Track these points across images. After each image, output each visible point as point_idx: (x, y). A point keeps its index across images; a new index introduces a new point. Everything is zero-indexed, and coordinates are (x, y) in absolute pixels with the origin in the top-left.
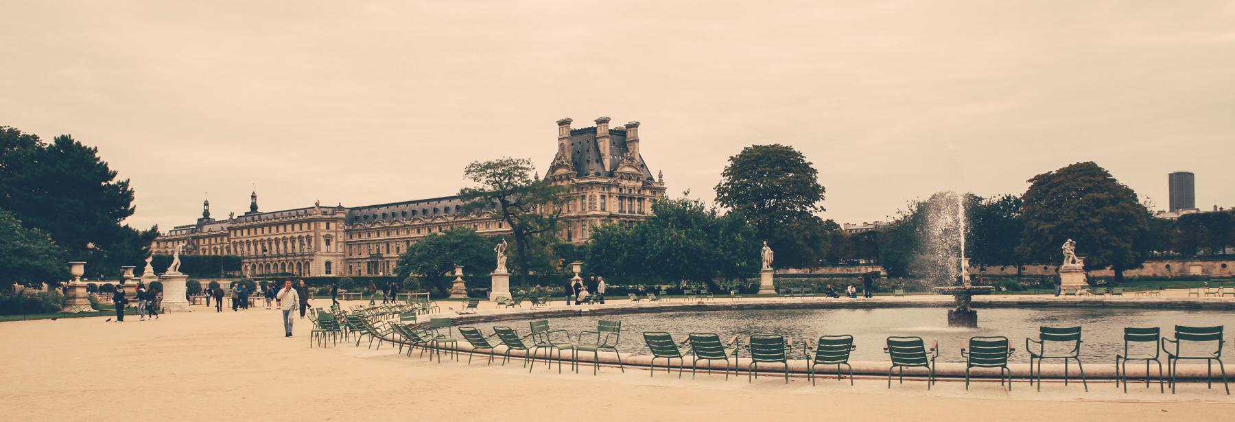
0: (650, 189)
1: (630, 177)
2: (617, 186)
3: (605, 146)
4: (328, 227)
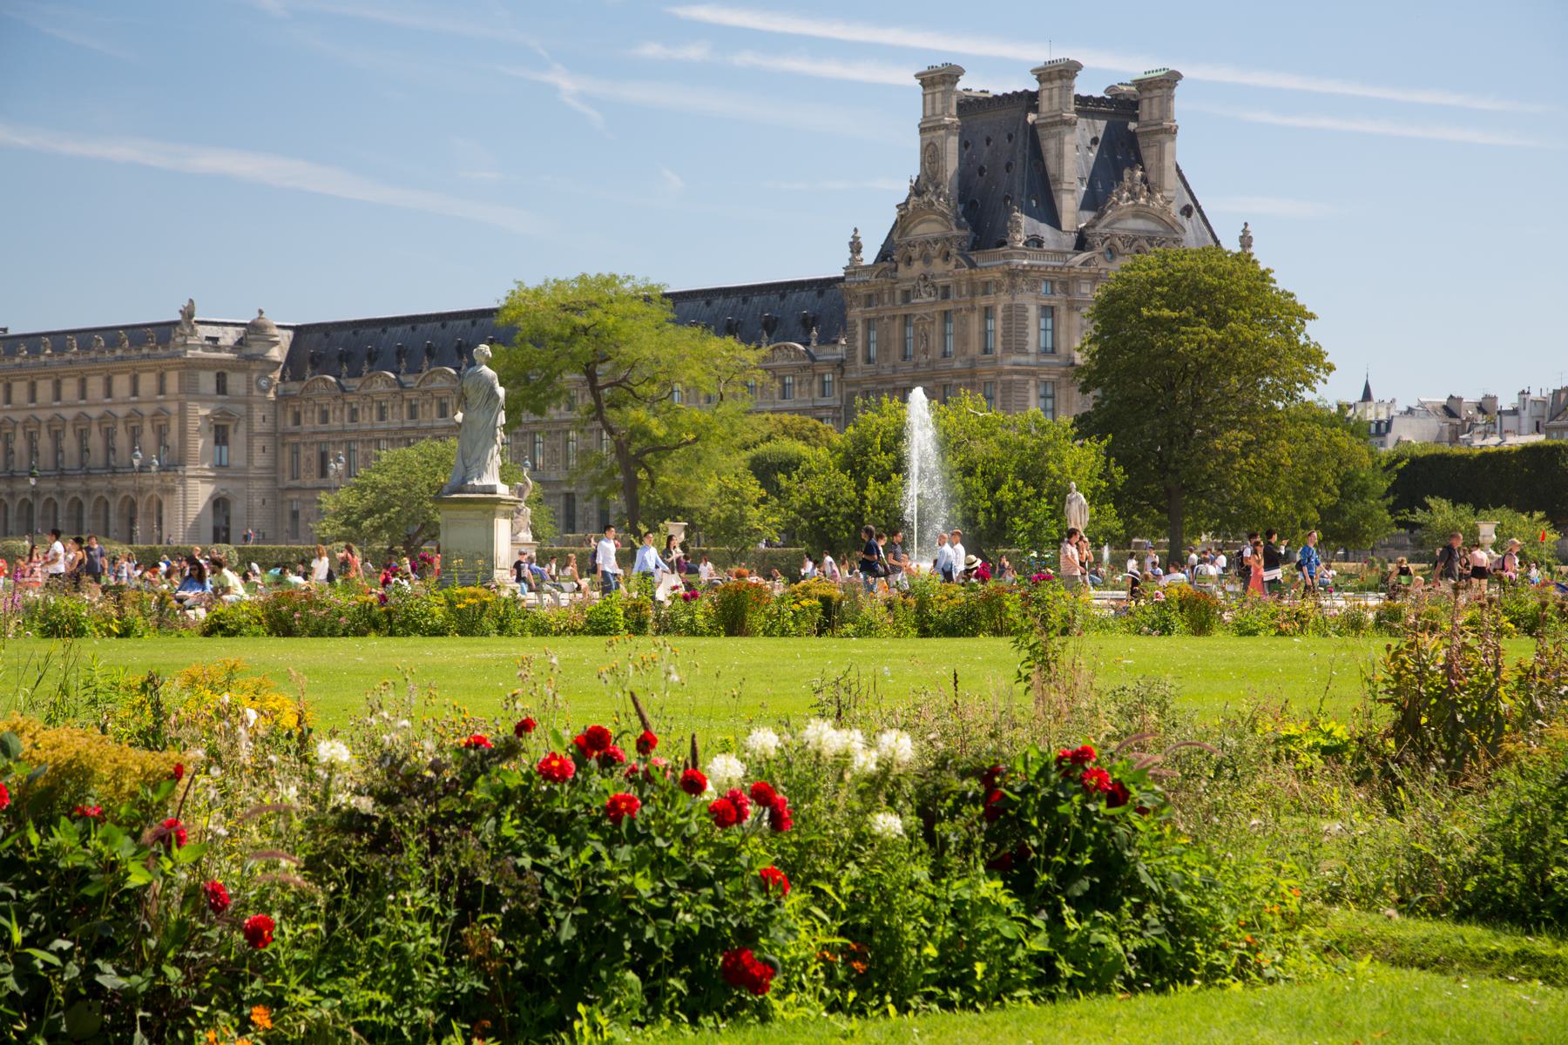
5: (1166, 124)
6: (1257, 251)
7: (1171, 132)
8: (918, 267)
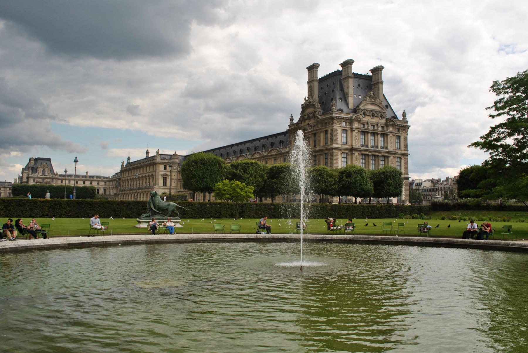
0: (393, 126)
1: (373, 114)
2: (359, 121)
3: (351, 86)
4: (165, 168)
5: (380, 81)
6: (408, 118)
7: (382, 83)
8: (307, 122)
